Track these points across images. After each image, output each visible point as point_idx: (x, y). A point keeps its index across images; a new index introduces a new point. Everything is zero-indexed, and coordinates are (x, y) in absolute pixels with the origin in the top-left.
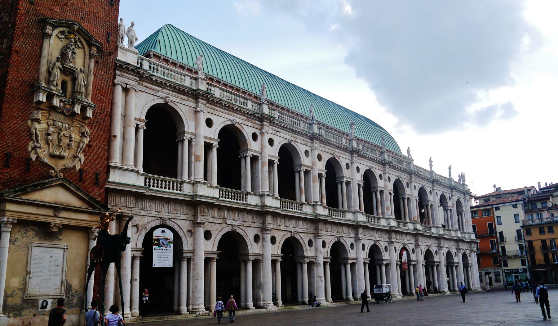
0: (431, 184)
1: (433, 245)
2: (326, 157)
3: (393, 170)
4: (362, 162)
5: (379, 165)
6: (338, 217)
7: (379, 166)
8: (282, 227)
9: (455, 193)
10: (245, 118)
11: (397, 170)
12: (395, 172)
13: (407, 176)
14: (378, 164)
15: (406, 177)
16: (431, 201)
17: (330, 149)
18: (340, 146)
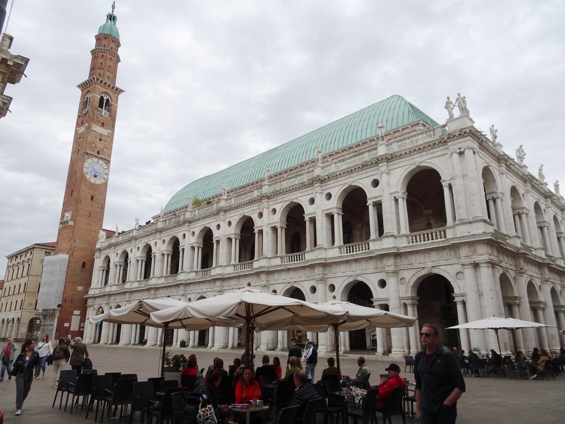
0: (312, 188)
1: (303, 279)
2: (167, 239)
3: (234, 211)
4: (196, 225)
5: (215, 217)
6: (168, 282)
7: (216, 218)
8: (136, 298)
9: (383, 167)
10: (128, 244)
11: (241, 208)
12: (237, 212)
13: (258, 205)
14: (213, 217)
15: (257, 207)
16: (308, 214)
17: (170, 232)
18: (174, 225)
